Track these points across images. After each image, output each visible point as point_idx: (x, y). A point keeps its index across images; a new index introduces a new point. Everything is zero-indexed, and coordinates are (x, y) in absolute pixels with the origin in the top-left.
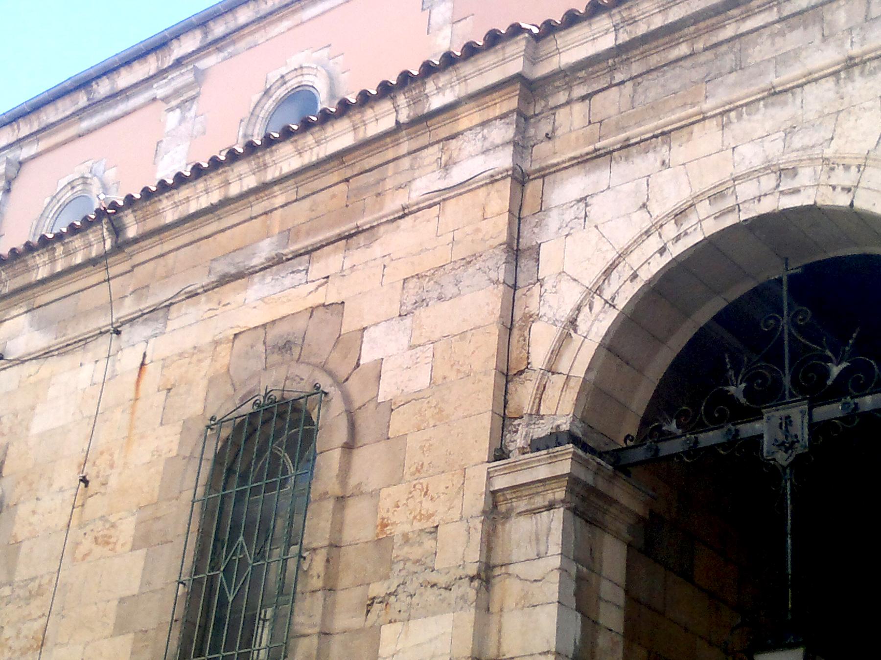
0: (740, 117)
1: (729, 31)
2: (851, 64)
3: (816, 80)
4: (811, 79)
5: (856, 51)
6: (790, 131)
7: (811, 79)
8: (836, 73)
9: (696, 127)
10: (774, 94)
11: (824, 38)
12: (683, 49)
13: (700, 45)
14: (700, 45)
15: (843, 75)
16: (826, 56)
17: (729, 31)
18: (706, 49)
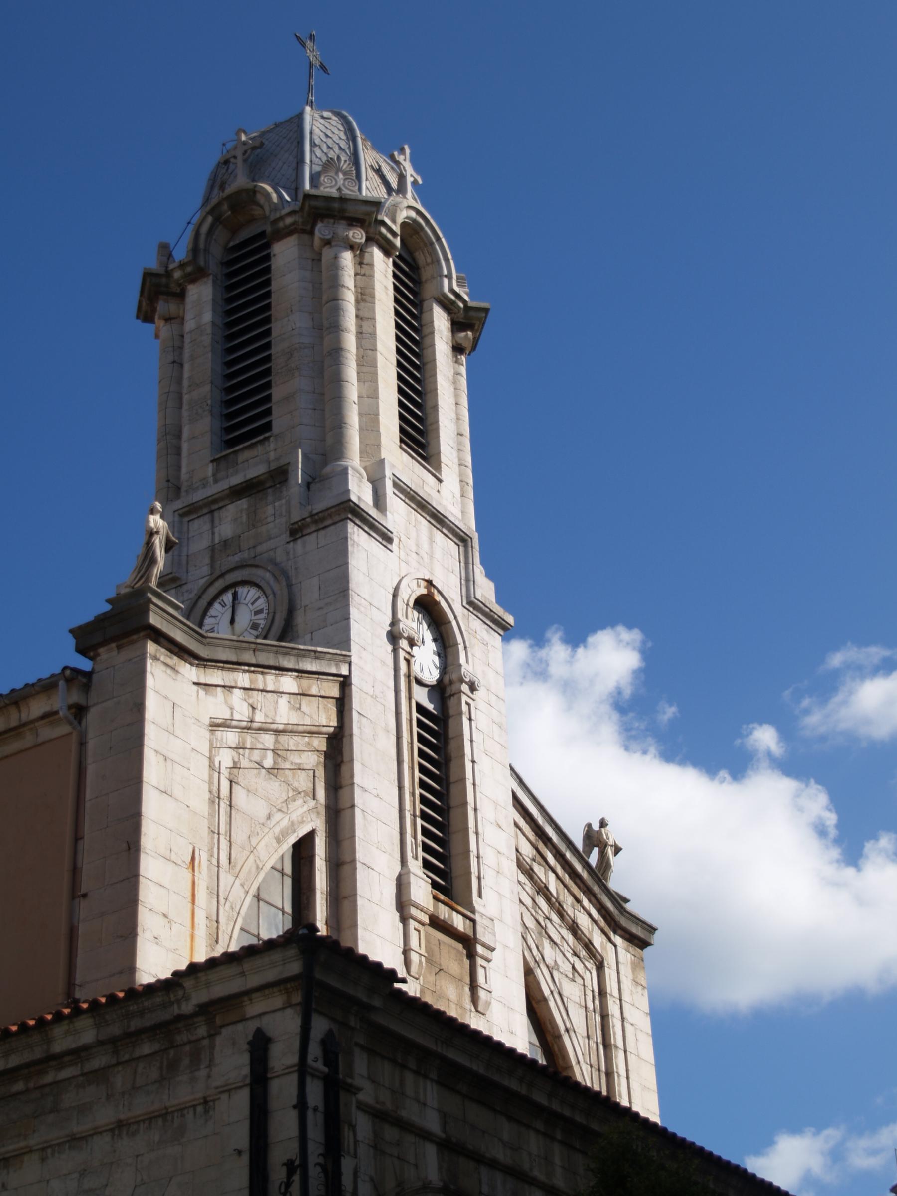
0: (53, 1154)
1: (49, 1078)
2: (120, 1127)
3: (101, 1133)
4: (97, 1132)
5: (122, 1117)
6: (83, 1173)
7: (97, 1132)
8: (112, 1130)
9: (26, 1158)
10: (75, 1141)
11: (108, 1097)
12: (20, 1086)
13: (31, 1085)
14: (31, 1085)
15: (116, 1132)
16: (105, 1116)
17: (49, 1078)
18: (36, 1088)
